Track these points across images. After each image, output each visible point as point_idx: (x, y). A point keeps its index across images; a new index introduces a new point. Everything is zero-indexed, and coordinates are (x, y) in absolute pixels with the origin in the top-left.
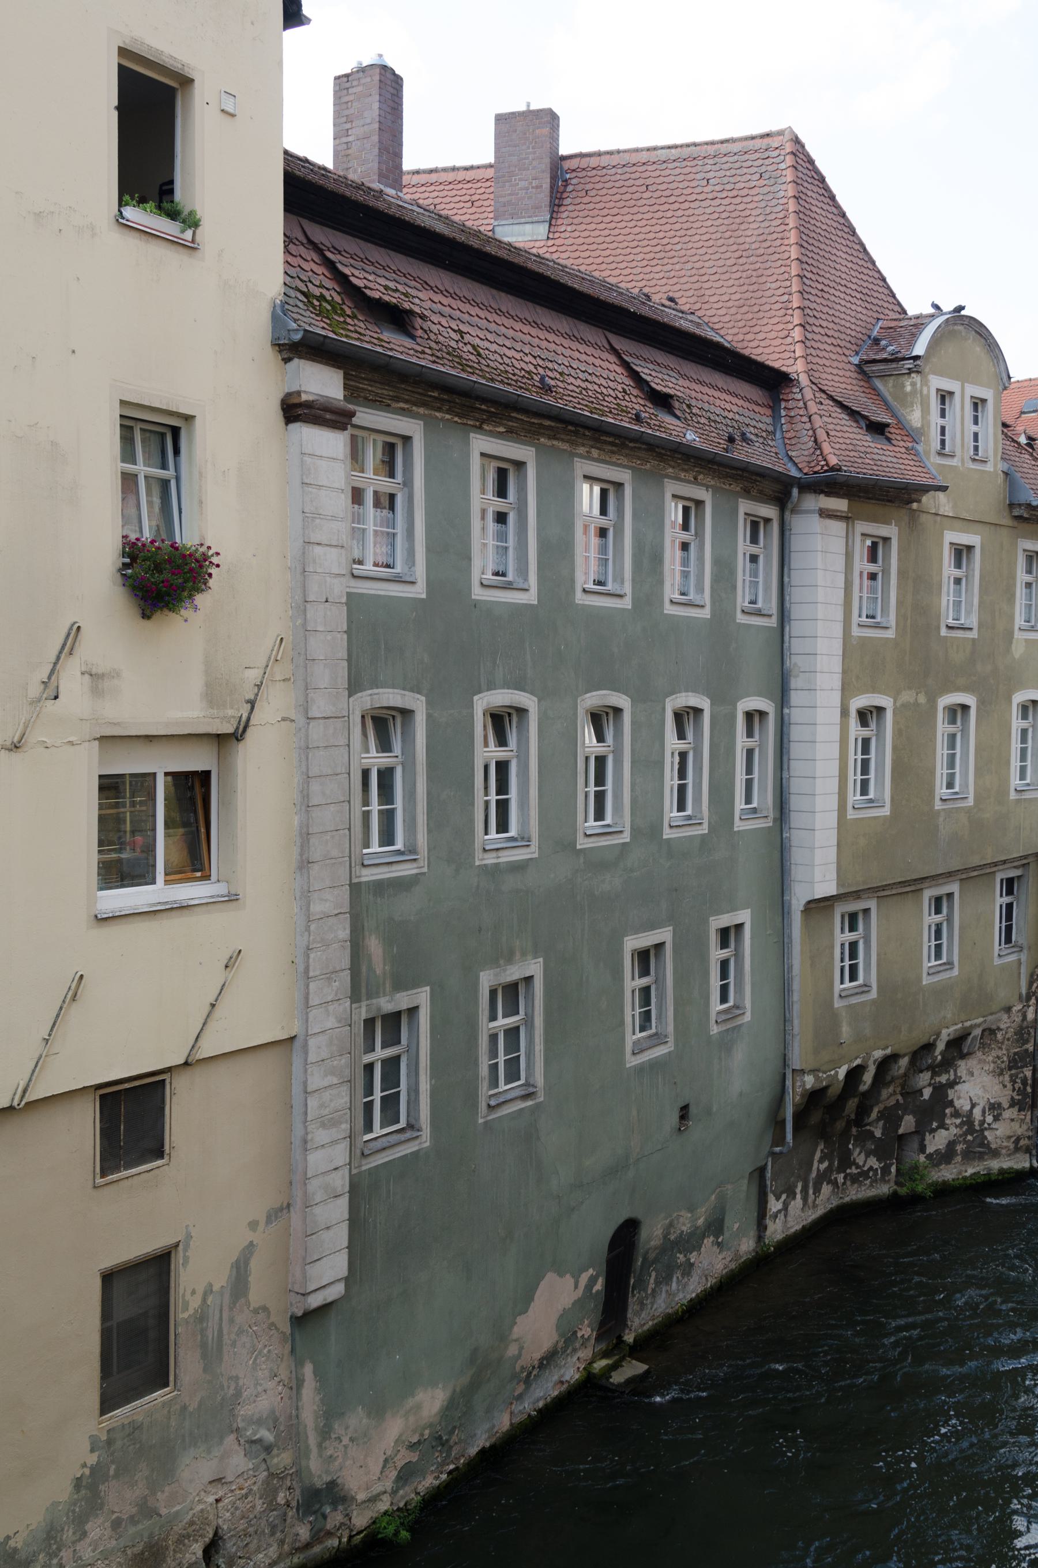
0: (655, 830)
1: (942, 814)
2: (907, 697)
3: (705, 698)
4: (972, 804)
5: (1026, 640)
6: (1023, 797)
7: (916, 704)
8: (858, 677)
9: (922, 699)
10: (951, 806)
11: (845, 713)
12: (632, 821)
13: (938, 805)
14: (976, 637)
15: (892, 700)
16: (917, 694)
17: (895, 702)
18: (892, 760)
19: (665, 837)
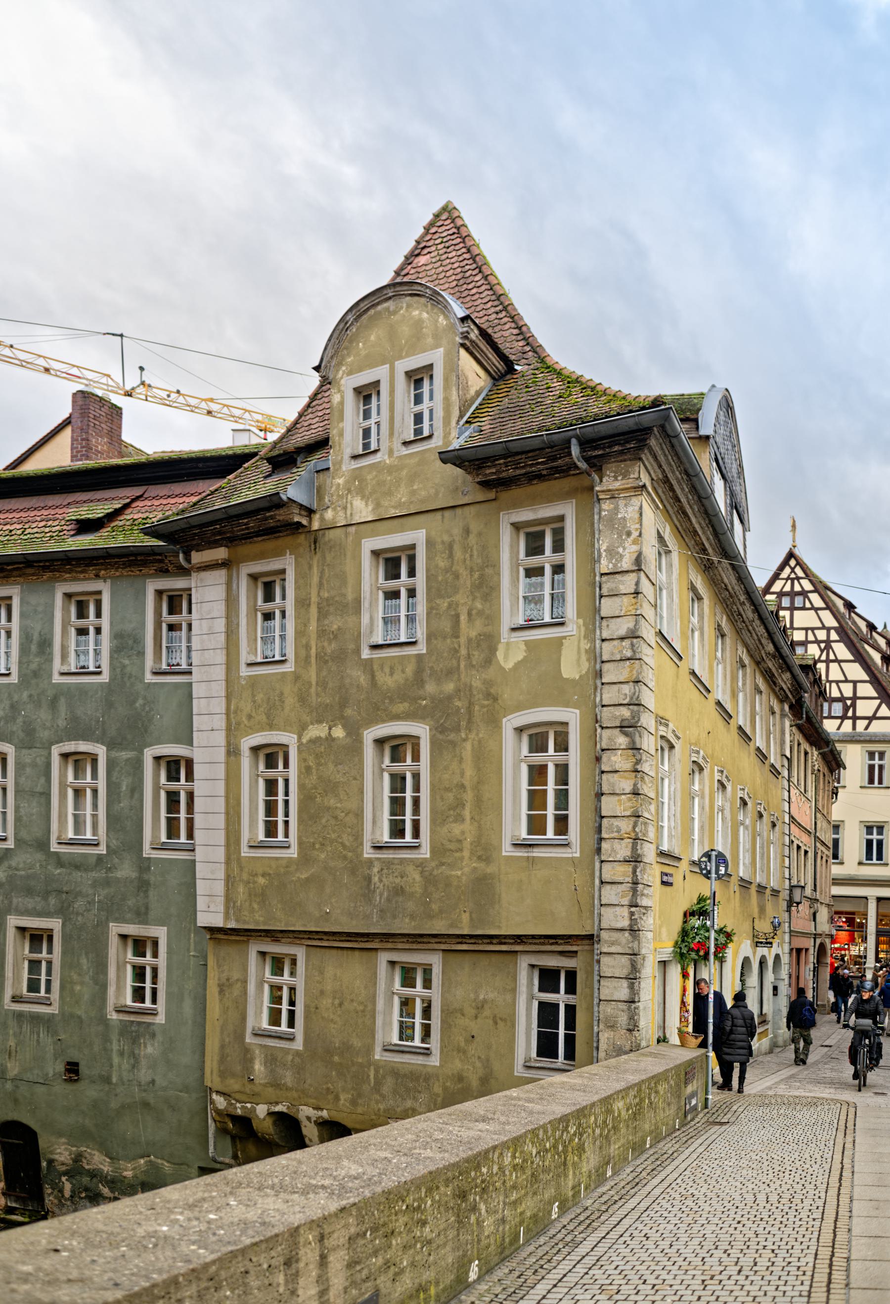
0: (43, 845)
1: (376, 863)
2: (317, 731)
3: (99, 745)
4: (428, 856)
5: (527, 643)
6: (530, 855)
7: (330, 738)
8: (250, 717)
9: (339, 732)
10: (391, 856)
11: (232, 752)
12: (15, 834)
13: (368, 853)
14: (424, 651)
15: (295, 736)
16: (330, 729)
17: (300, 738)
18: (299, 799)
19: (52, 850)
